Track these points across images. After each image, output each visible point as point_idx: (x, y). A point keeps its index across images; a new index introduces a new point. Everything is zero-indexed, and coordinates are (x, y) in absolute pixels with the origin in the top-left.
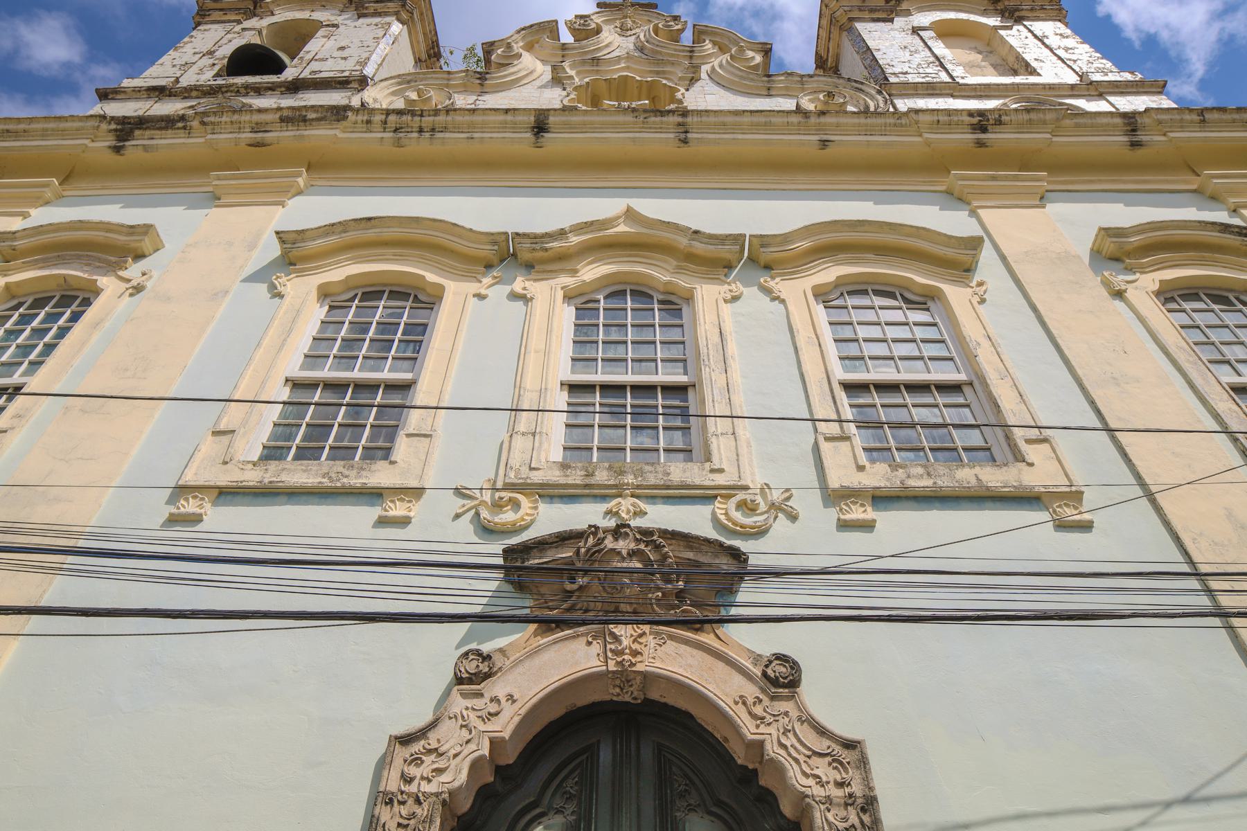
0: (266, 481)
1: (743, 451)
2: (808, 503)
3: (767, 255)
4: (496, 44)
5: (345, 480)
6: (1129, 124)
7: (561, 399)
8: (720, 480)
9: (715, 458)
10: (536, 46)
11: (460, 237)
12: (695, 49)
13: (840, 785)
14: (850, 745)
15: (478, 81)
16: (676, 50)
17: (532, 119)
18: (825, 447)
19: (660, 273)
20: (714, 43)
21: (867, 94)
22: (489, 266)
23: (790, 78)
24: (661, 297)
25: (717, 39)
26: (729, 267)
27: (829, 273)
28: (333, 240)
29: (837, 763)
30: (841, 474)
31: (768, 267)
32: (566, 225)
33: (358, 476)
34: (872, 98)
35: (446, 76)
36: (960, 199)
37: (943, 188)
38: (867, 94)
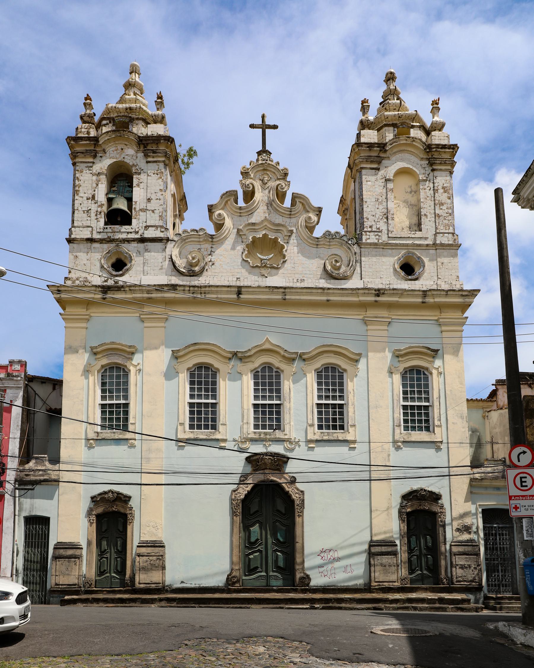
0: (195, 437)
1: (291, 429)
2: (303, 444)
3: (305, 357)
4: (213, 206)
5: (211, 437)
6: (424, 295)
7: (252, 410)
8: (286, 437)
9: (285, 431)
10: (229, 202)
11: (222, 350)
12: (292, 210)
13: (300, 497)
14: (302, 492)
15: (210, 240)
16: (285, 210)
17: (237, 290)
18: (308, 428)
19: (275, 361)
20: (300, 202)
21: (351, 252)
22: (230, 359)
23: (326, 239)
24: (276, 370)
25: (302, 201)
26: (294, 360)
27: (319, 363)
28: (187, 350)
29: (299, 495)
30: (310, 436)
31: (304, 360)
32: (250, 348)
33: (213, 436)
34: (353, 256)
35: (198, 236)
36: (365, 323)
37: (361, 317)
38: (351, 252)
